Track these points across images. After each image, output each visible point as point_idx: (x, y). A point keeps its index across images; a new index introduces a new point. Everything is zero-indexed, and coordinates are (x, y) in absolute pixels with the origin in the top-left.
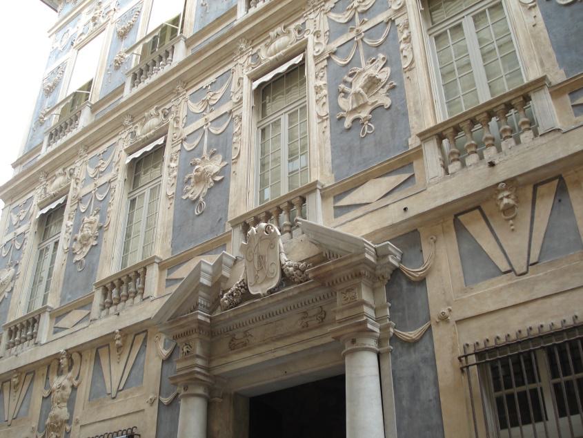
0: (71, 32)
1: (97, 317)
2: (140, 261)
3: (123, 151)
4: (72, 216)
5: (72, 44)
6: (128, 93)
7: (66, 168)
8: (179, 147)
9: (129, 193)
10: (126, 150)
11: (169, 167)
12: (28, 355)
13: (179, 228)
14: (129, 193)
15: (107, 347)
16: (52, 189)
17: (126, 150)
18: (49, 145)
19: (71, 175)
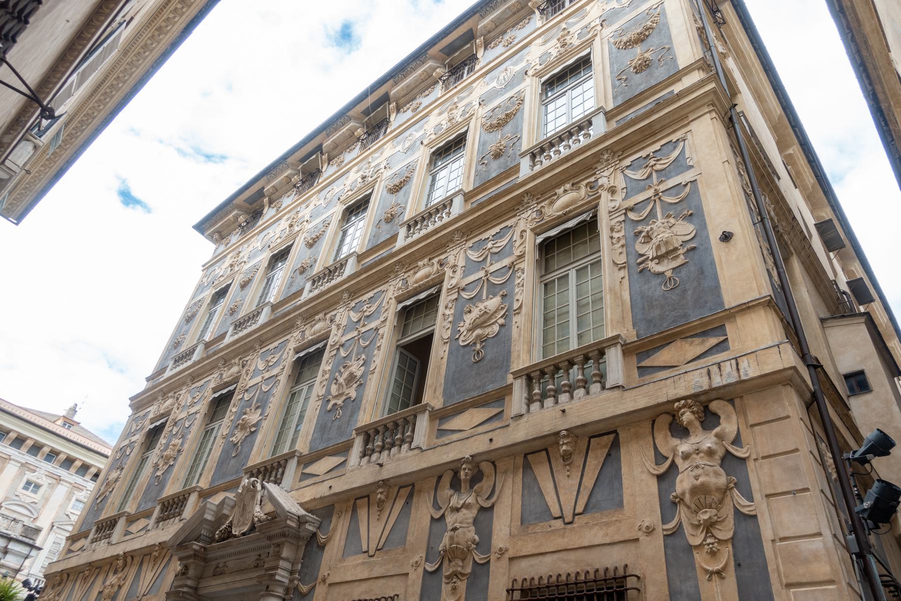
0: (337, 190)
1: (524, 411)
2: (576, 347)
3: (528, 231)
4: (450, 305)
5: (339, 199)
6: (400, 243)
7: (433, 258)
8: (455, 296)
9: (541, 277)
10: (532, 230)
11: (612, 238)
12: (401, 462)
13: (642, 306)
14: (541, 277)
15: (544, 452)
16: (309, 336)
17: (532, 230)
18: (407, 237)
19: (332, 321)
